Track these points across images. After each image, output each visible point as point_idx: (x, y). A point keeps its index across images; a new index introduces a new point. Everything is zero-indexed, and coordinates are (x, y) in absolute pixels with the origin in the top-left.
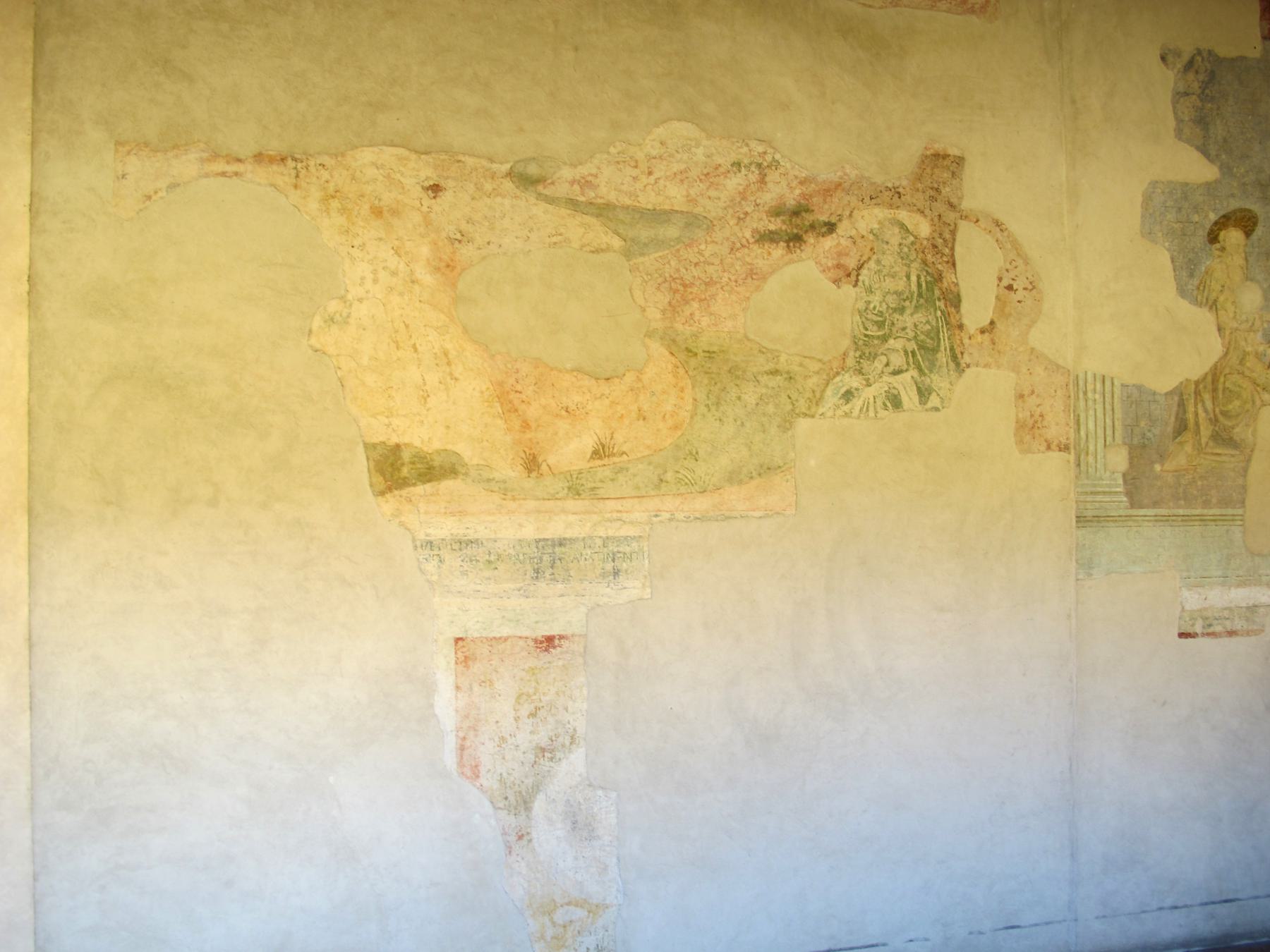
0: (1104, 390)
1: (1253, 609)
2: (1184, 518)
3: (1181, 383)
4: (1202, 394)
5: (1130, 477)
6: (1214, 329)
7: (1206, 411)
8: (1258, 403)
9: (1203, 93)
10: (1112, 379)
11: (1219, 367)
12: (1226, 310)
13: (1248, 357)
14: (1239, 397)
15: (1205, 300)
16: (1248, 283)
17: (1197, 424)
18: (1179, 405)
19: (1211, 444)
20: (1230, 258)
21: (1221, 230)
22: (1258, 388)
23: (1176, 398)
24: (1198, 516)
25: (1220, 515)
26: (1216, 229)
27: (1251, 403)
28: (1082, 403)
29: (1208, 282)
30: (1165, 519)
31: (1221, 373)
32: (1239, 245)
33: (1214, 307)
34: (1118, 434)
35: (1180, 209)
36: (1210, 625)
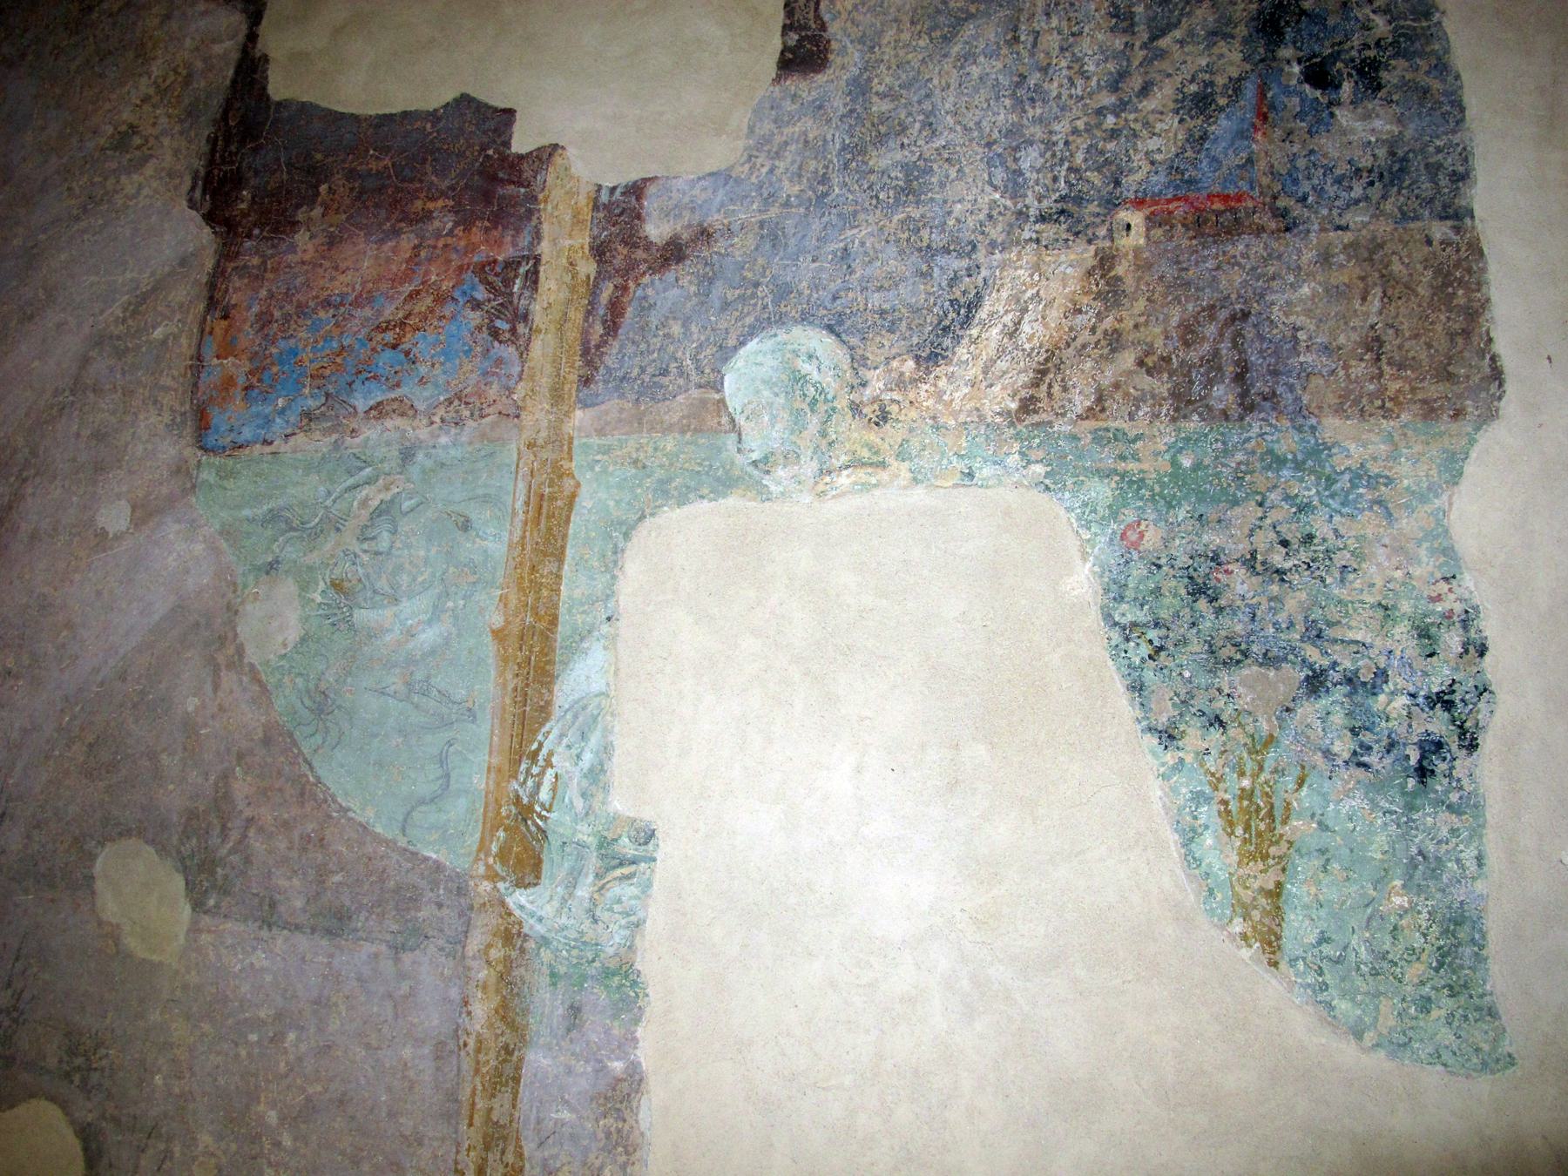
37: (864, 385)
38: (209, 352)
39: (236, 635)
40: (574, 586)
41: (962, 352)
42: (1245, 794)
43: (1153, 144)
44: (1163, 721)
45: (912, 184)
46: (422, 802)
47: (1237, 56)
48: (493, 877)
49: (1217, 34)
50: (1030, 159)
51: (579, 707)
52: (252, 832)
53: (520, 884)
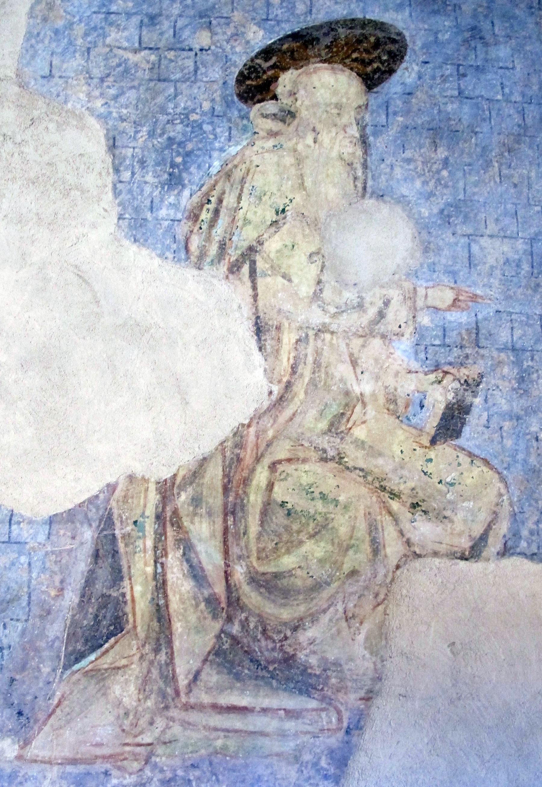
3: (112, 488)
4: (186, 523)
11: (252, 438)
12: (284, 277)
15: (213, 250)
16: (369, 203)
18: (96, 556)
20: (309, 140)
21: (285, 69)
22: (395, 505)
26: (265, 65)
27: (366, 547)
29: (230, 200)
31: (258, 459)
32: (339, 106)
33: (246, 269)
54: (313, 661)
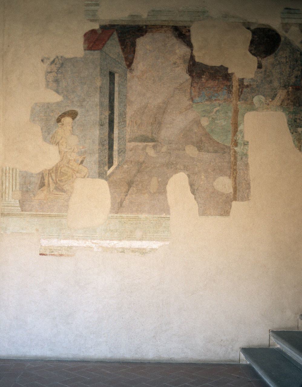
0: (13, 173)
1: (71, 247)
2: (42, 215)
3: (43, 170)
5: (21, 201)
6: (58, 152)
7: (52, 179)
8: (75, 177)
9: (58, 71)
10: (16, 169)
13: (71, 161)
14: (66, 174)
15: (54, 142)
17: (49, 184)
19: (54, 191)
22: (75, 172)
23: (41, 176)
24: (48, 215)
25: (57, 215)
28: (4, 177)
29: (56, 136)
30: (36, 215)
31: (59, 167)
34: (18, 187)
35: (46, 112)
36: (52, 252)
37: (267, 101)
38: (192, 91)
39: (200, 123)
40: (239, 119)
41: (275, 99)
42: (298, 138)
43: (292, 81)
44: (292, 132)
45: (271, 82)
46: (225, 140)
47: (300, 73)
48: (233, 146)
49: (299, 70)
50: (282, 81)
51: (241, 130)
52: (205, 143)
53: (236, 147)
54: (65, 189)
